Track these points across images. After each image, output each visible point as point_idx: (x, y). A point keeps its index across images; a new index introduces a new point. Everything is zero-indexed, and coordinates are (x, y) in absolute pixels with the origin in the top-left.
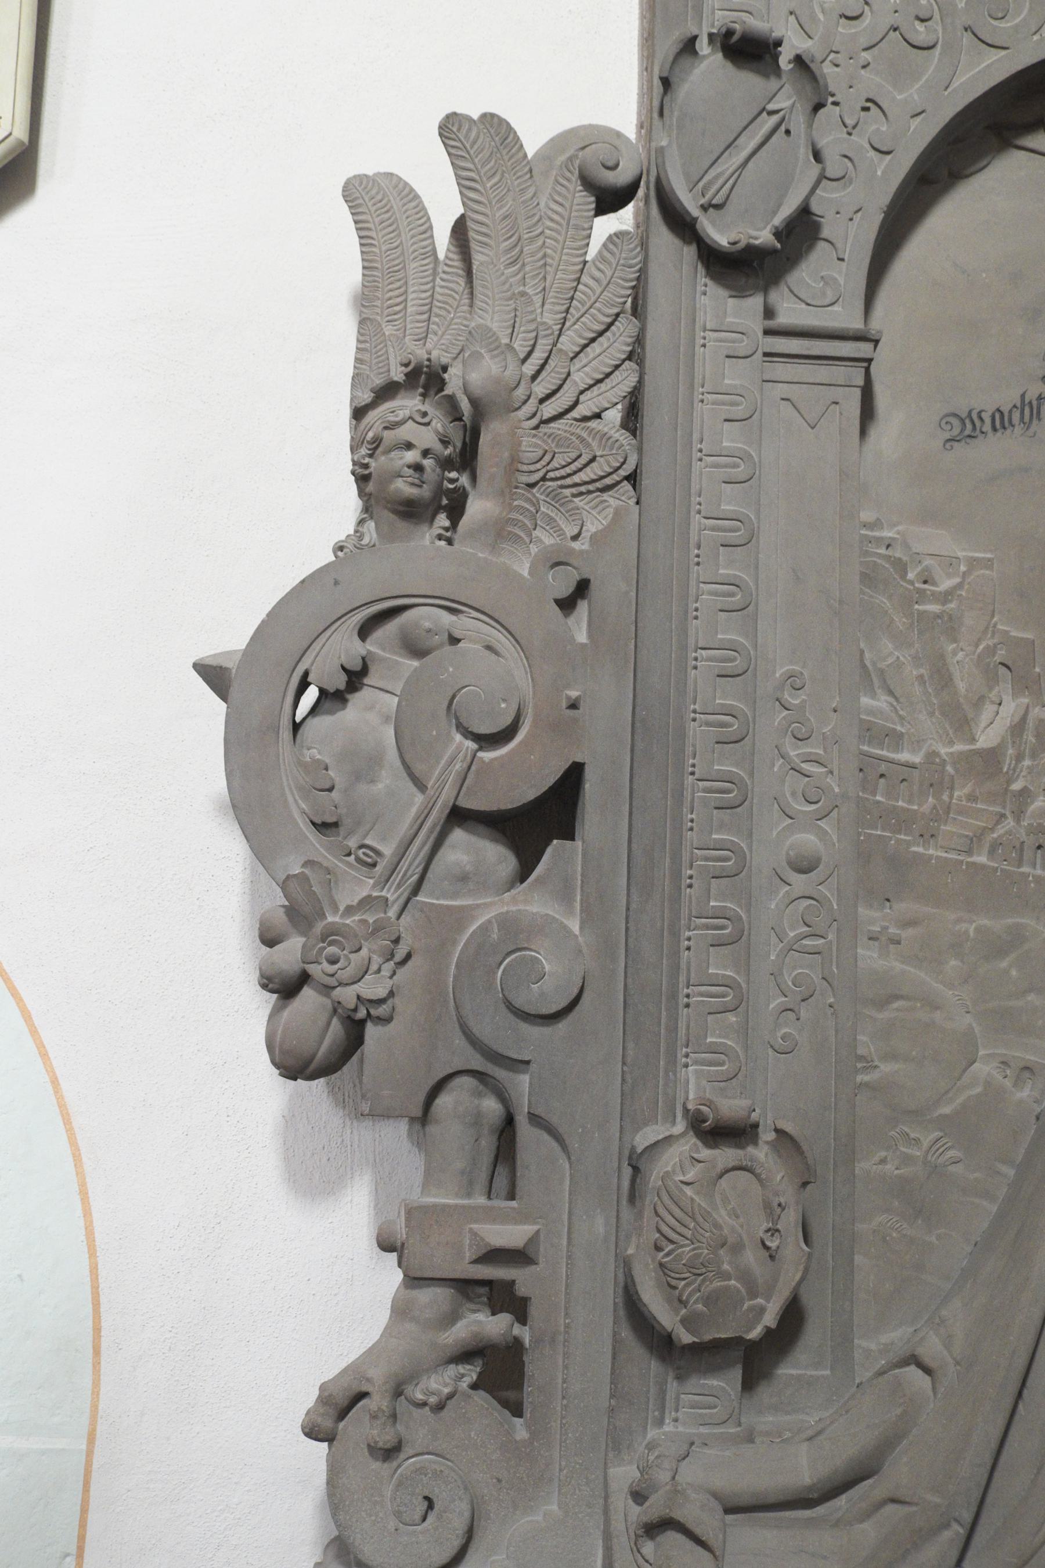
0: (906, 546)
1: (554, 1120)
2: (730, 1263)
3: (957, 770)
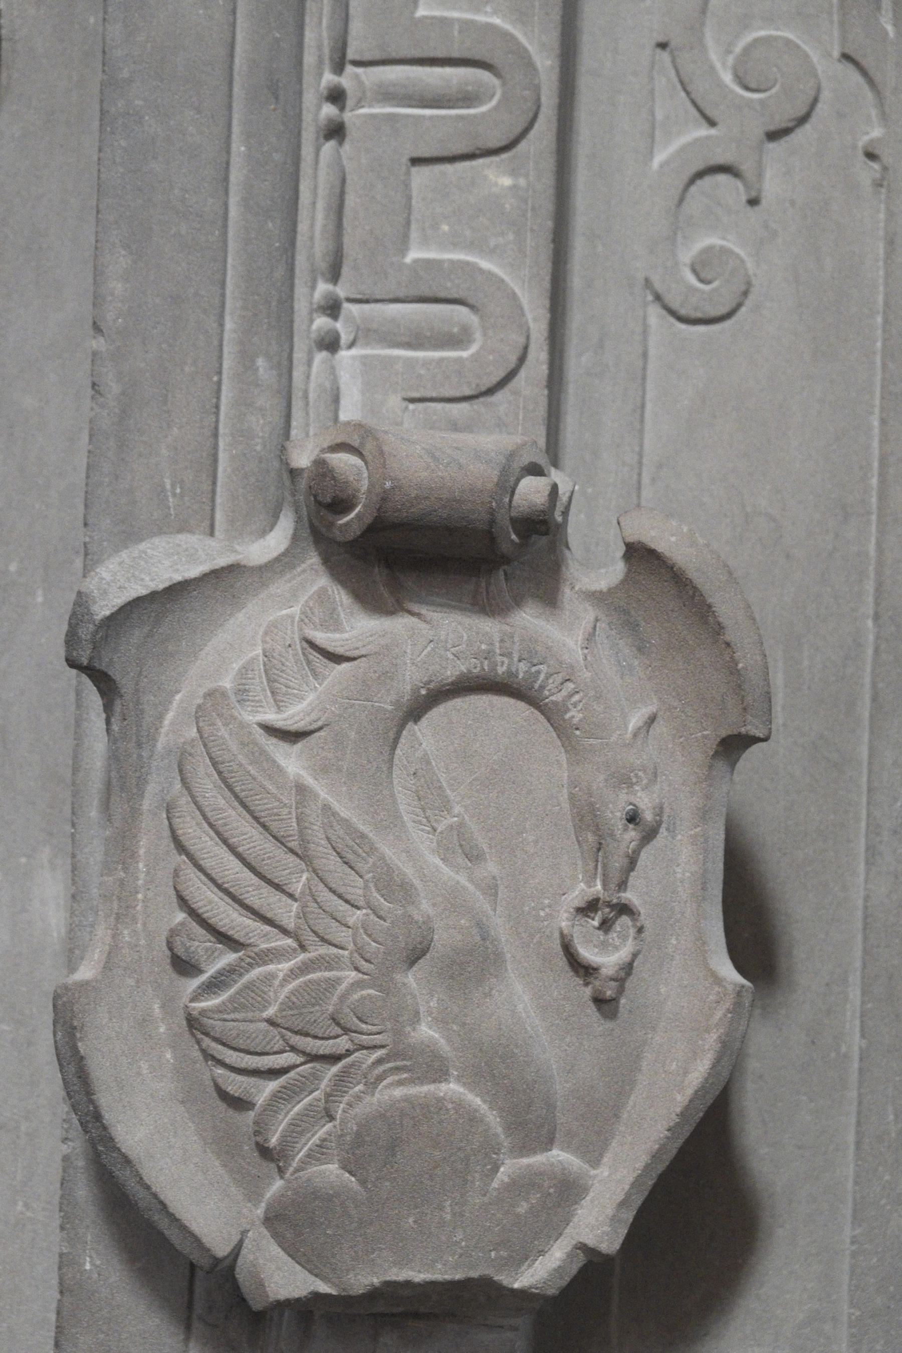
2: (442, 1021)
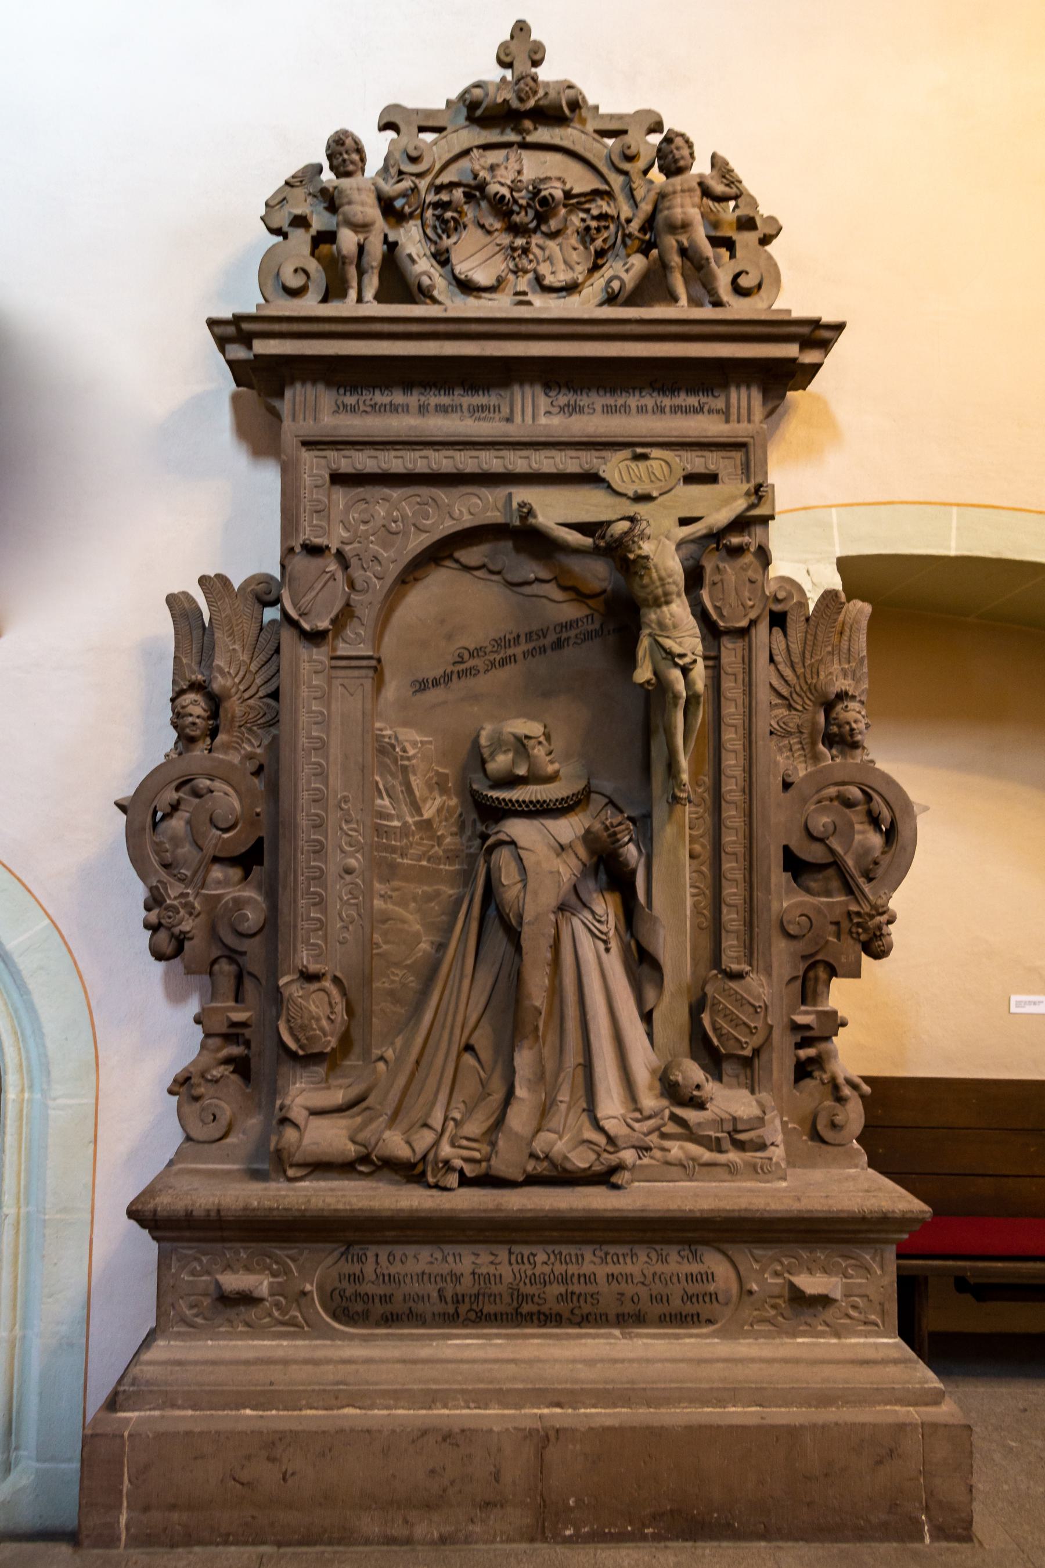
0: (396, 738)
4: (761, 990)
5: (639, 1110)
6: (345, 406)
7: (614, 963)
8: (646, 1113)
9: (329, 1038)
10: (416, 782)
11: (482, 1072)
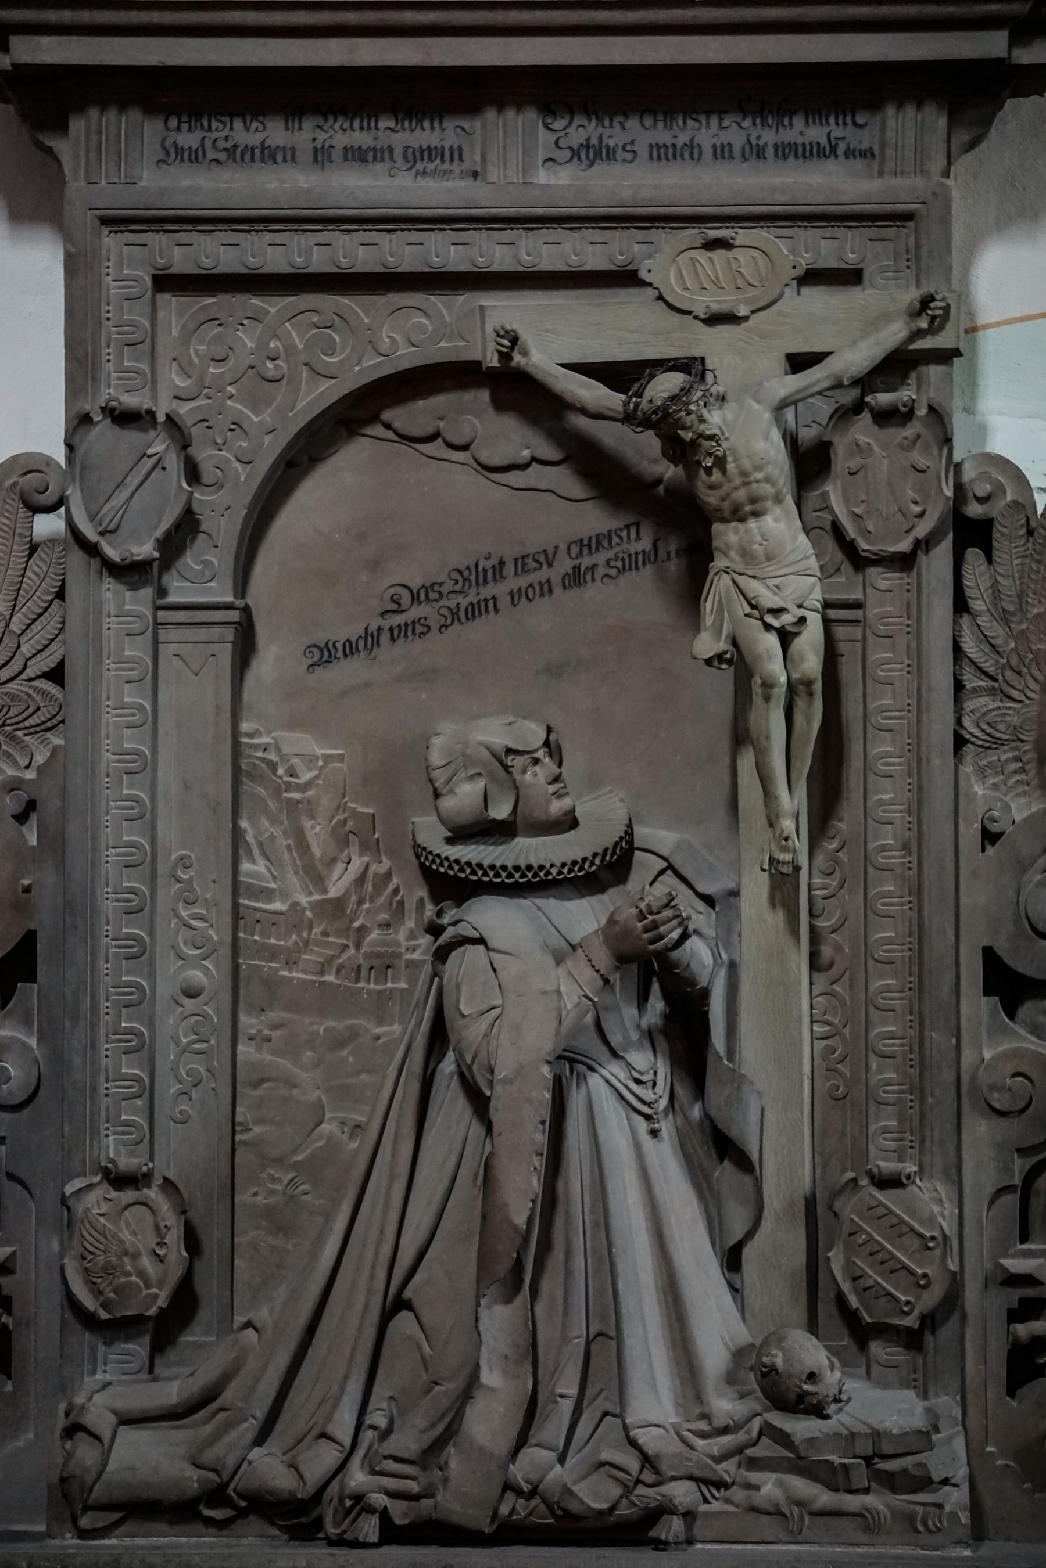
0: (278, 750)
1: (22, 1176)
2: (132, 1266)
3: (314, 914)
4: (936, 1209)
5: (705, 1416)
6: (179, 151)
7: (665, 1158)
8: (719, 1422)
9: (154, 1290)
10: (316, 832)
11: (426, 1348)
